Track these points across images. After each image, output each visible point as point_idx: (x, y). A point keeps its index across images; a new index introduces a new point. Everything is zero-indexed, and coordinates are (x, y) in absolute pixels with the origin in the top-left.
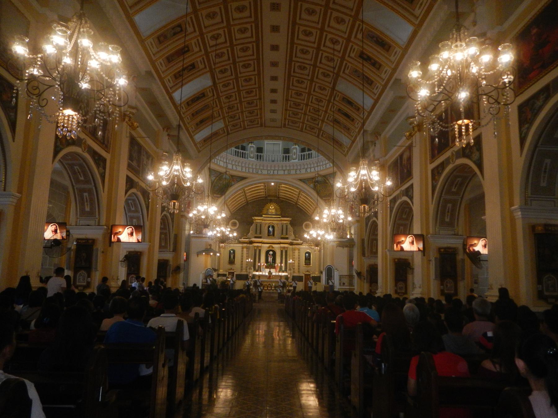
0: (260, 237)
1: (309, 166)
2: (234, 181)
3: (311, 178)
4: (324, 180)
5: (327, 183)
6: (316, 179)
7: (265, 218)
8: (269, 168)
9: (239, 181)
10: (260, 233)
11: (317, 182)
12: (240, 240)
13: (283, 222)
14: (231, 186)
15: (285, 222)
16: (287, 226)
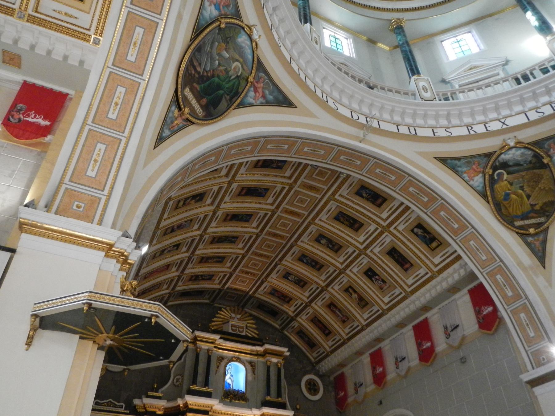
0: (208, 395)
1: (481, 118)
2: (256, 91)
3: (480, 155)
4: (537, 156)
5: (545, 166)
6: (503, 156)
7: (222, 341)
8: (355, 106)
9: (268, 103)
10: (206, 384)
11: (505, 165)
12: (137, 402)
13: (268, 357)
14: (242, 105)
15: (274, 360)
16: (279, 370)
